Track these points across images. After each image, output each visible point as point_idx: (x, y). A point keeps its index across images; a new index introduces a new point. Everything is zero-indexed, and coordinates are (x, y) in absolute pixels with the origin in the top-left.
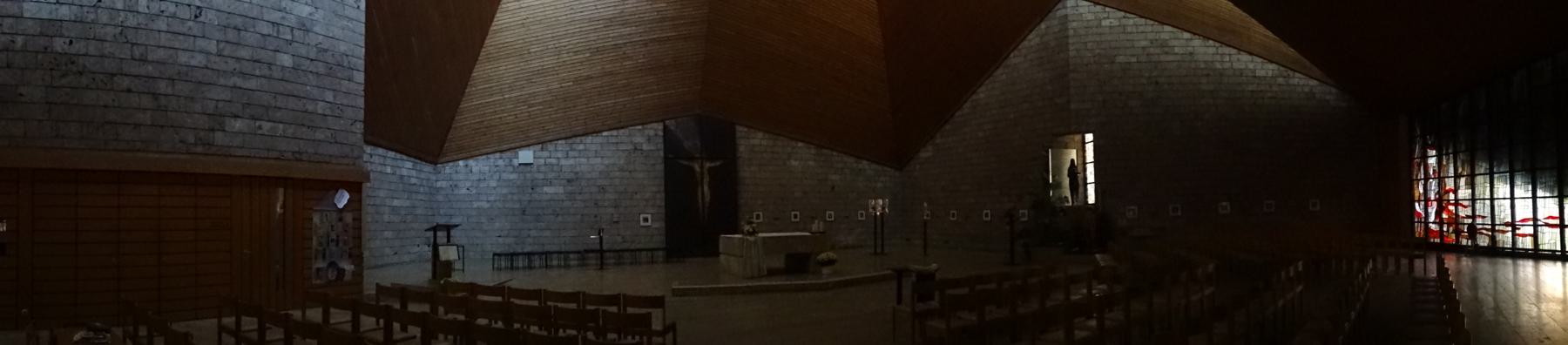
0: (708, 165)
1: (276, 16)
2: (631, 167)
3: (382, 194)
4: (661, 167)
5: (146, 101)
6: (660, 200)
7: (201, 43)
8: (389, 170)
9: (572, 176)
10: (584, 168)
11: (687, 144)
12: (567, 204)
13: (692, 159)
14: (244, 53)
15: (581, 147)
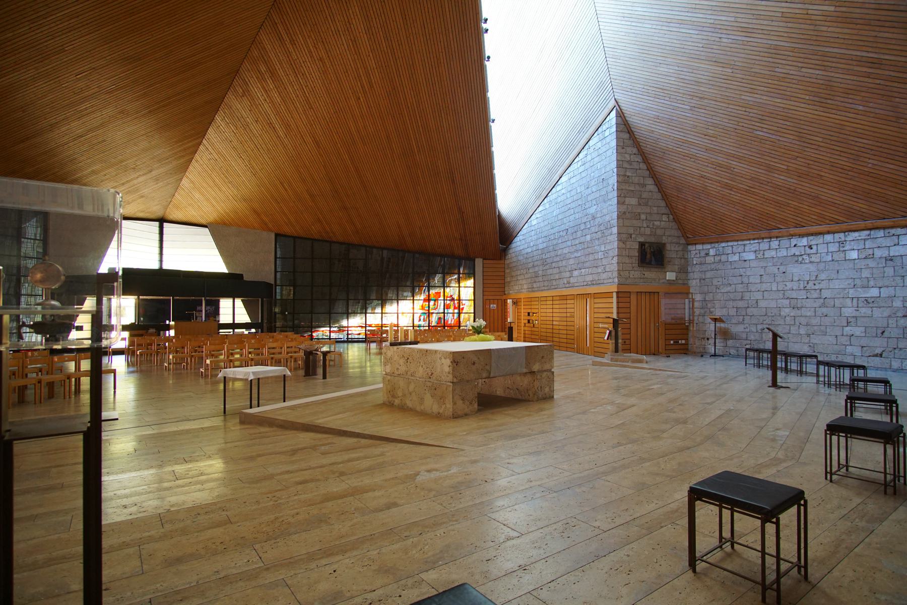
3: (836, 284)
8: (854, 255)
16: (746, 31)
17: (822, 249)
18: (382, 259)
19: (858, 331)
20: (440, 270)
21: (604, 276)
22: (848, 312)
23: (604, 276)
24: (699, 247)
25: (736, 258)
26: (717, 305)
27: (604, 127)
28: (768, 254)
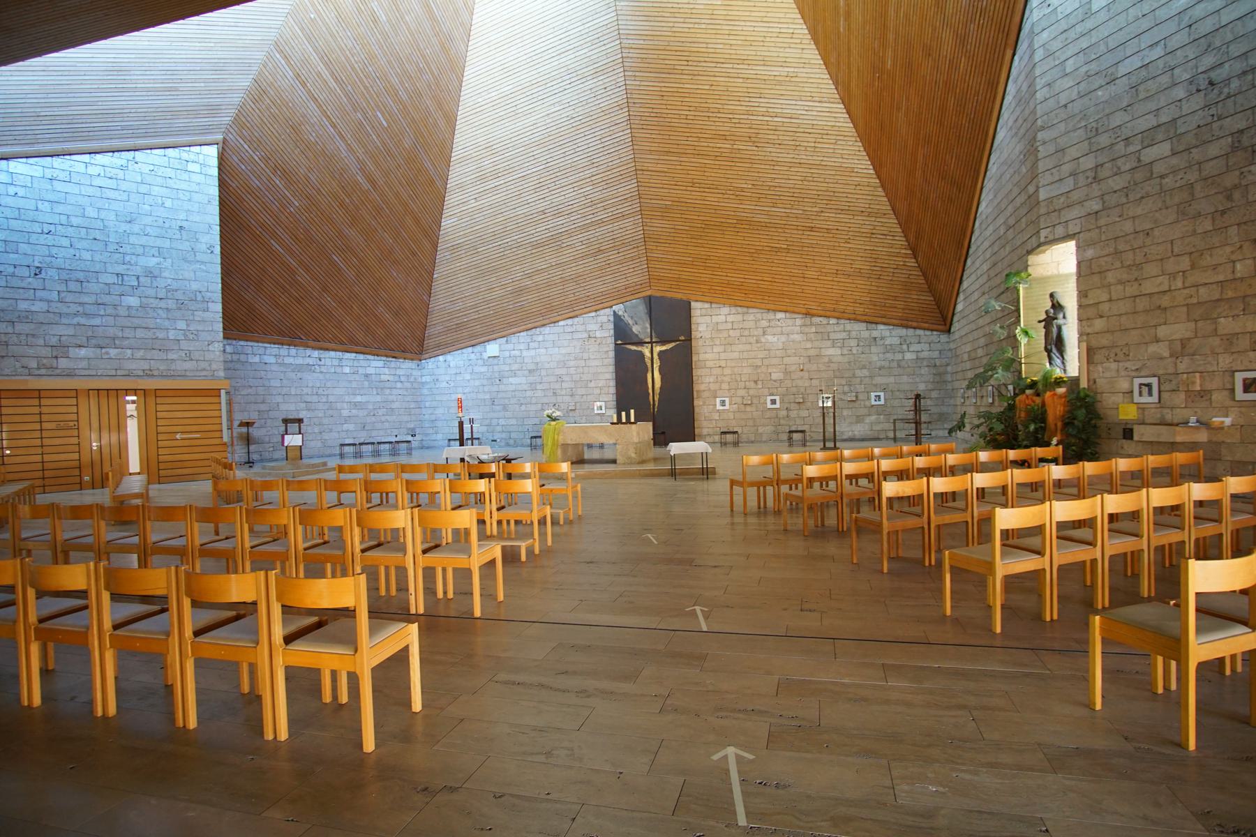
0: (658, 349)
1: (121, 269)
2: (585, 356)
4: (612, 354)
6: (613, 390)
9: (532, 367)
11: (635, 329)
12: (529, 394)
13: (641, 343)
14: (86, 299)
15: (540, 338)
17: (328, 362)
19: (351, 427)
22: (345, 413)
23: (188, 365)
25: (257, 359)
27: (184, 153)
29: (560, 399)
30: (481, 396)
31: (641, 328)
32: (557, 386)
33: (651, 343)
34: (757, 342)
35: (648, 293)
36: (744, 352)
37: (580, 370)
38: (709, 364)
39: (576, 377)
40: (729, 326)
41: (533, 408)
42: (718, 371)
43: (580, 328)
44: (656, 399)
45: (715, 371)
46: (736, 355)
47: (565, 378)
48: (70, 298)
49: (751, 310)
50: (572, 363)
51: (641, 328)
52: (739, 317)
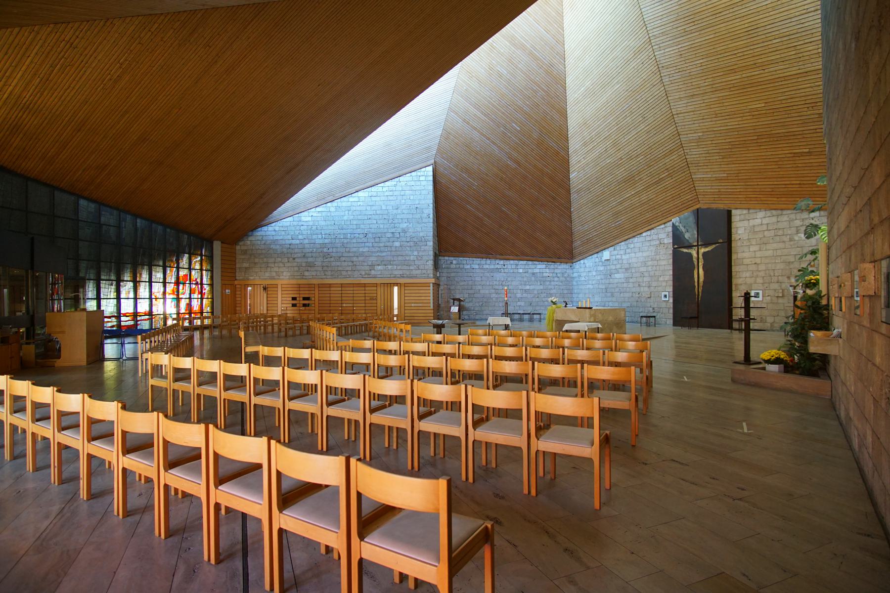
0: (702, 250)
1: (393, 230)
5: (350, 264)
7: (367, 244)
9: (627, 266)
10: (634, 260)
11: (687, 236)
12: (625, 285)
13: (690, 246)
14: (381, 245)
15: (632, 246)
16: (517, 162)
17: (509, 267)
18: (136, 229)
19: (522, 304)
20: (187, 250)
21: (418, 272)
22: (519, 295)
23: (418, 272)
24: (446, 258)
25: (468, 267)
26: (457, 291)
27: (419, 173)
28: (485, 267)
29: (642, 289)
30: (601, 286)
31: (690, 235)
32: (641, 280)
33: (698, 245)
34: (791, 240)
35: (698, 206)
36: (771, 251)
37: (654, 268)
38: (746, 261)
39: (652, 273)
40: (765, 227)
41: (627, 295)
42: (754, 267)
43: (655, 237)
44: (700, 291)
45: (754, 267)
46: (770, 253)
47: (646, 274)
48: (376, 245)
49: (785, 212)
50: (650, 263)
51: (690, 235)
52: (774, 219)
